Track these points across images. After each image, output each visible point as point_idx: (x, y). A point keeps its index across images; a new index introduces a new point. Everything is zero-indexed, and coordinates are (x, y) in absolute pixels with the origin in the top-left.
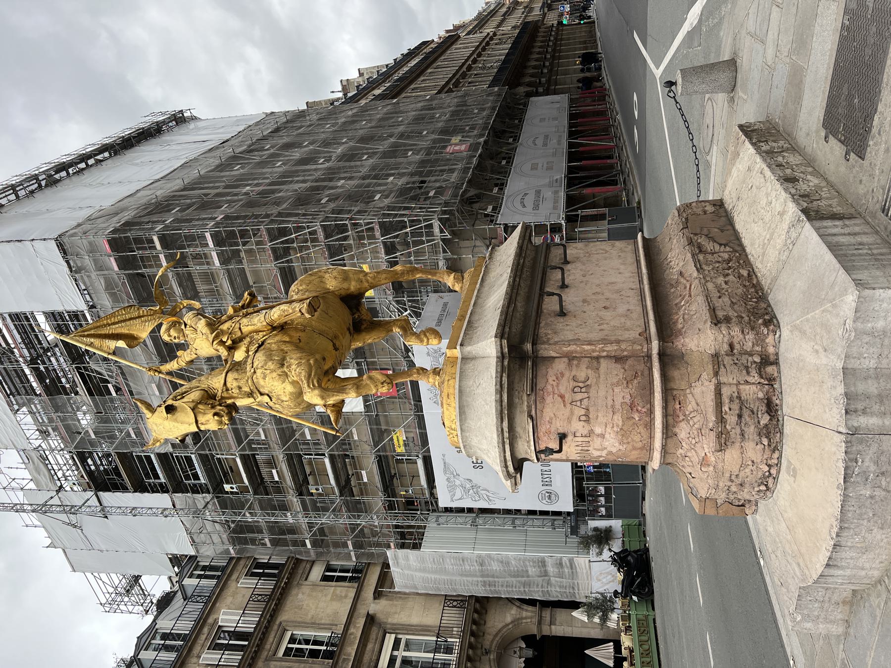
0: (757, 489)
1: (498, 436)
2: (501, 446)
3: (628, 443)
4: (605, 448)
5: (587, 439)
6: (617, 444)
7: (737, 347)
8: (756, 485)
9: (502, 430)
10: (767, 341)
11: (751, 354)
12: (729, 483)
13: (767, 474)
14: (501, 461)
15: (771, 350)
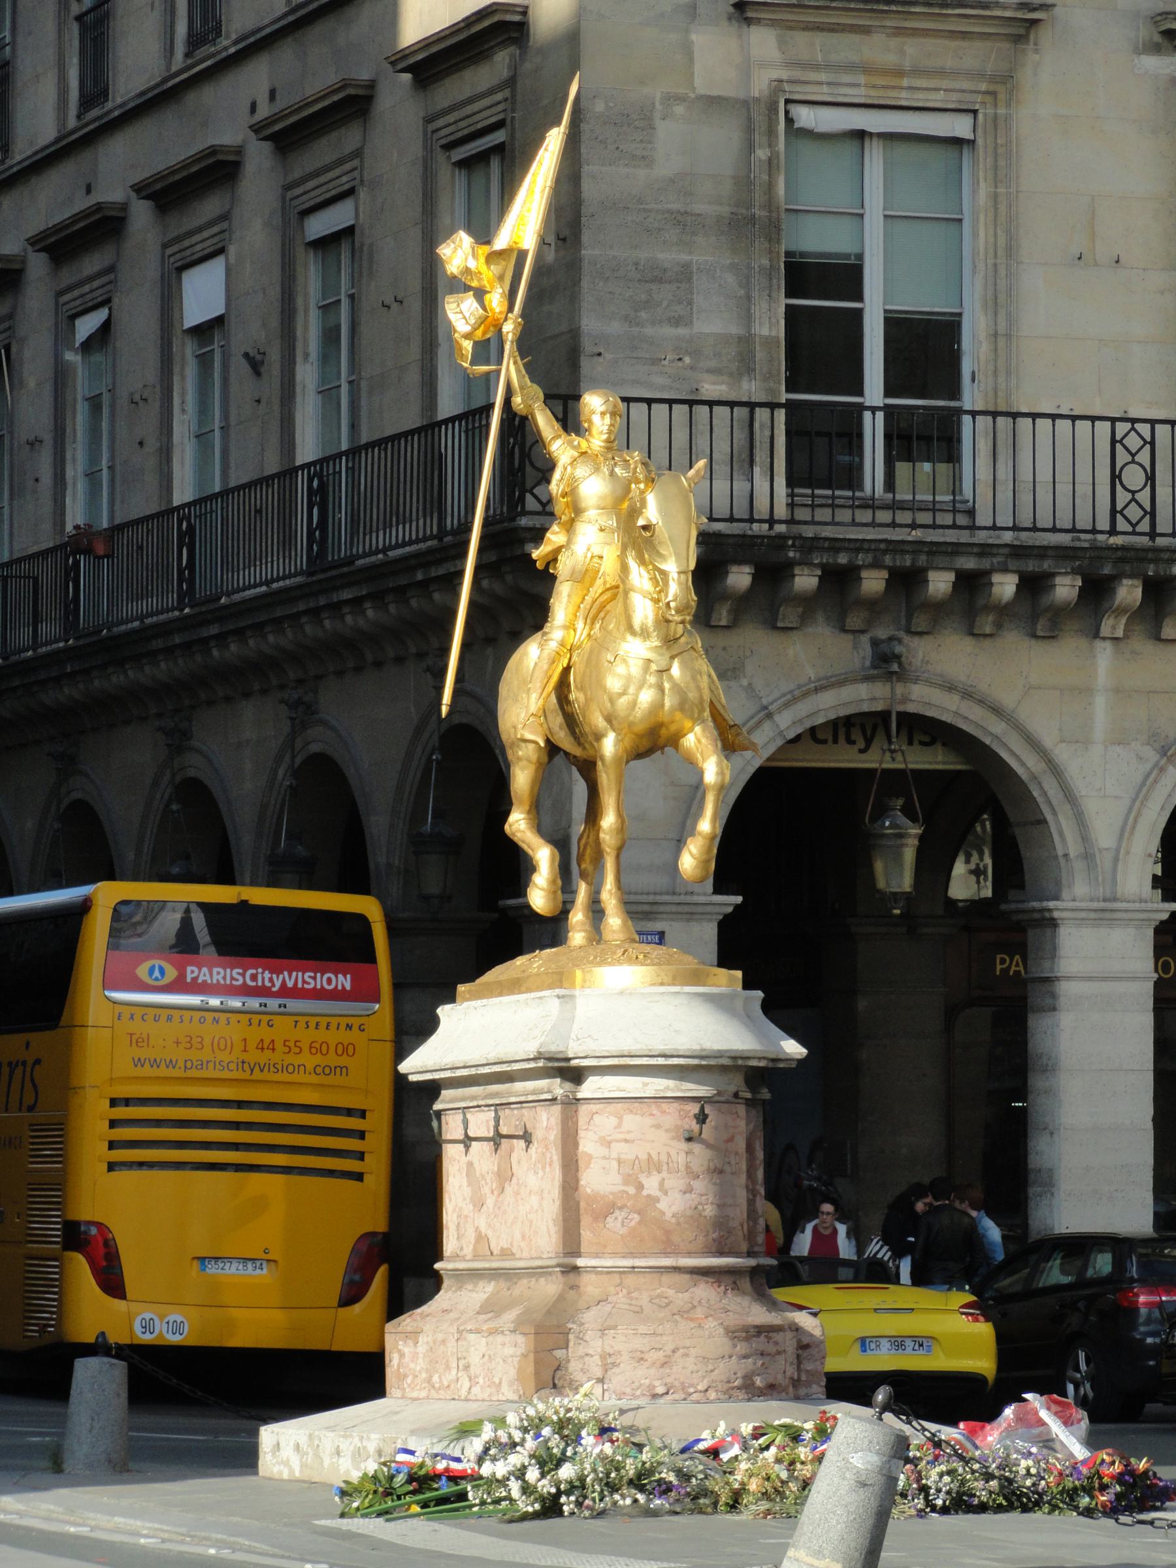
0: (657, 1383)
1: (719, 1051)
2: (704, 1054)
3: (679, 1224)
4: (666, 1193)
5: (682, 1168)
6: (675, 1209)
7: (805, 1354)
8: (669, 1380)
9: (721, 1057)
10: (814, 1386)
11: (799, 1369)
12: (669, 1347)
13: (692, 1390)
14: (676, 1050)
15: (802, 1391)
